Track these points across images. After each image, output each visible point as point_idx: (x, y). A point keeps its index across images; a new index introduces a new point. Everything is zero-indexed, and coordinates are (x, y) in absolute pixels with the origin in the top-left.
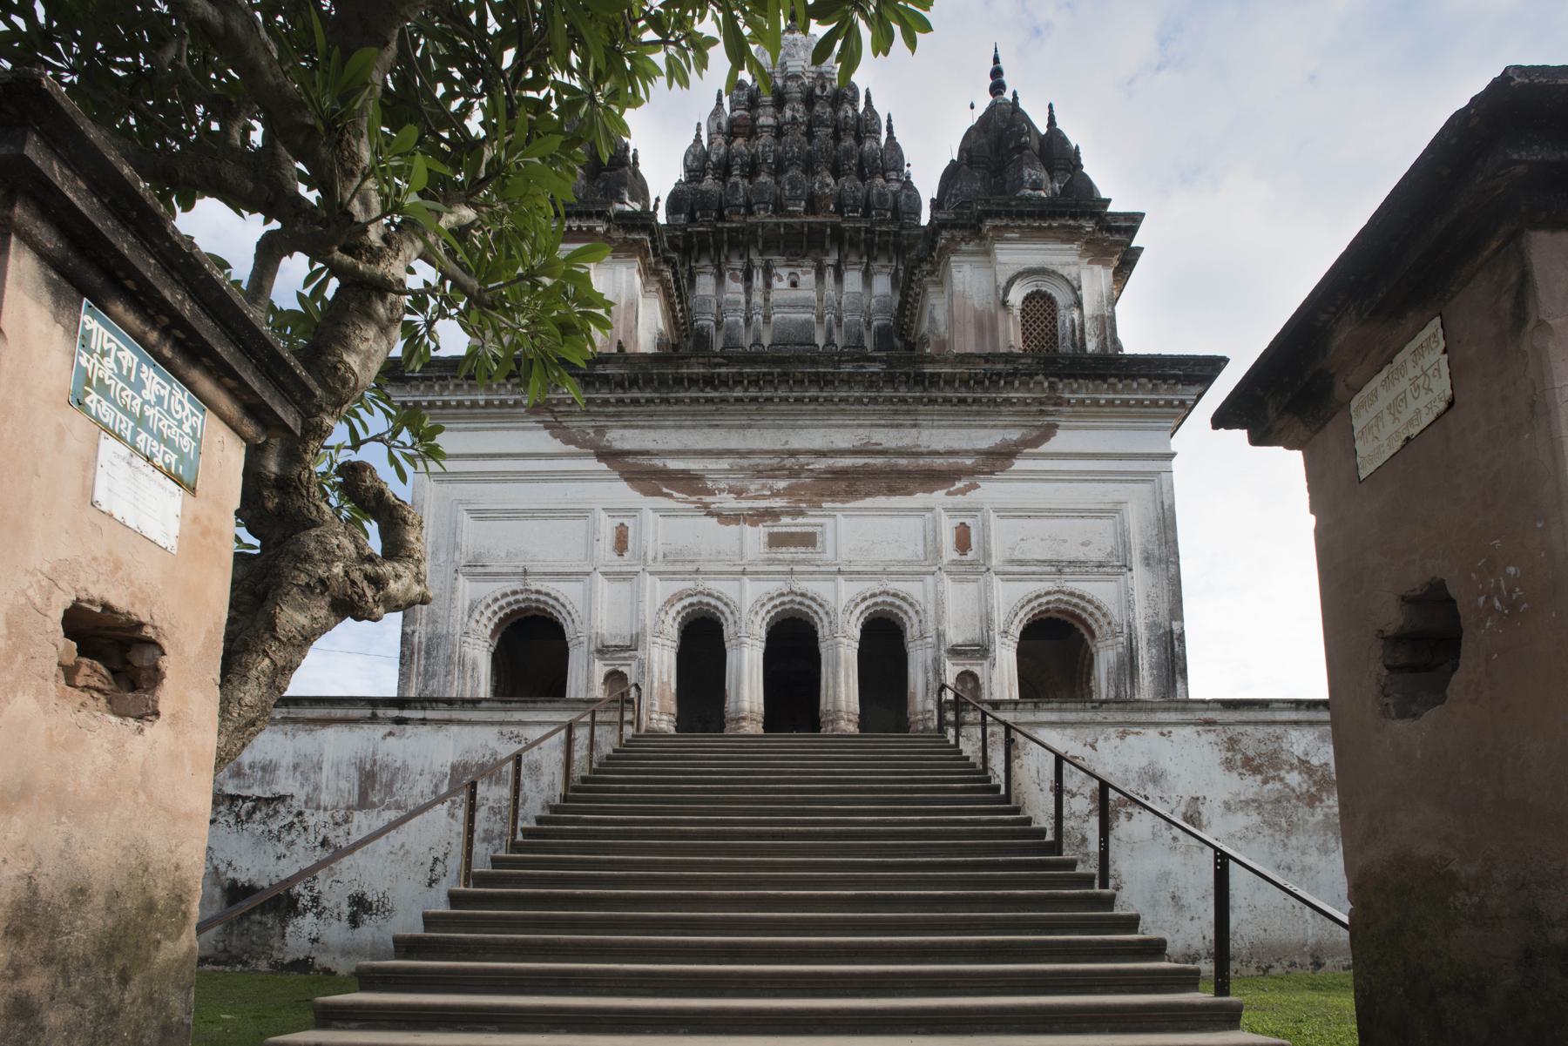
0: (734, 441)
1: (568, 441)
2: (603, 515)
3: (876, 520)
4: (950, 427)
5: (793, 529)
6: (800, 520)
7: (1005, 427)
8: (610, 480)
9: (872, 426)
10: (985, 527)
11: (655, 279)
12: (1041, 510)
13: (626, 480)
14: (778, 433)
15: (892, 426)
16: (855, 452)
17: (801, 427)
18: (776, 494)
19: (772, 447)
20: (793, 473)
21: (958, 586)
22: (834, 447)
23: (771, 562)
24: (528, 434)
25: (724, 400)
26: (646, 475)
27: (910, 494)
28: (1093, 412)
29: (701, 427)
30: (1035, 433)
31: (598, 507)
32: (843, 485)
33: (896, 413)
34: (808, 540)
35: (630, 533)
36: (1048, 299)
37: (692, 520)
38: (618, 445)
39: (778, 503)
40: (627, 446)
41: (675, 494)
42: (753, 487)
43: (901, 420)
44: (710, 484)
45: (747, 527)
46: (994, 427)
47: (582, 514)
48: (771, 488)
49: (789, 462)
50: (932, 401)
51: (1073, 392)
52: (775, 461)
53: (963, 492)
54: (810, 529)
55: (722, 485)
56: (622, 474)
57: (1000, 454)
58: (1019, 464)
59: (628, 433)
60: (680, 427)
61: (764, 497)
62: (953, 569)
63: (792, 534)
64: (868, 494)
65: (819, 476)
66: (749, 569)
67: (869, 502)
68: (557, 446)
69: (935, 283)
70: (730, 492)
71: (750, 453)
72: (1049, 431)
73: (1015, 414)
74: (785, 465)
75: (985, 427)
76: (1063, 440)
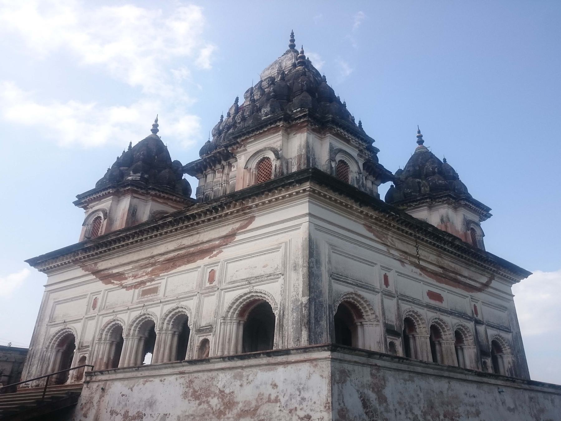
3: (180, 276)
4: (211, 230)
5: (151, 287)
7: (233, 223)
8: (97, 281)
12: (245, 256)
13: (101, 280)
18: (147, 274)
21: (206, 299)
23: (139, 303)
32: (171, 264)
39: (146, 277)
41: (115, 282)
42: (140, 273)
46: (228, 225)
53: (215, 255)
54: (156, 286)
56: (100, 278)
58: (238, 238)
62: (204, 291)
64: (180, 266)
65: (162, 263)
66: (130, 307)
75: (225, 225)
76: (257, 223)
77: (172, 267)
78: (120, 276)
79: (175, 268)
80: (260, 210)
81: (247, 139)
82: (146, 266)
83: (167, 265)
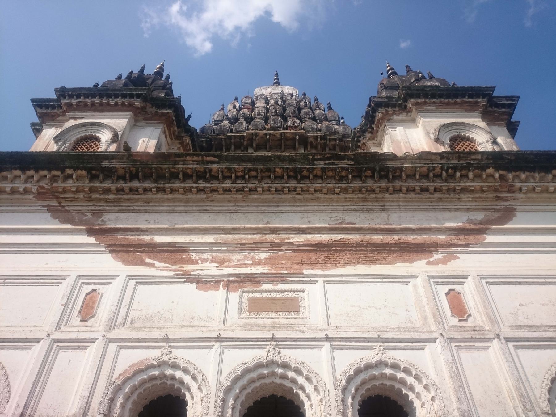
4: (415, 211)
5: (274, 295)
6: (281, 286)
7: (468, 210)
9: (345, 210)
15: (362, 211)
20: (273, 246)
29: (192, 211)
33: (365, 200)
43: (369, 205)
44: (193, 255)
46: (457, 210)
48: (253, 258)
49: (270, 238)
50: (396, 191)
52: (257, 237)
54: (292, 295)
60: (173, 211)
61: (246, 266)
63: (273, 300)
64: (347, 264)
65: (297, 248)
70: (212, 261)
72: (507, 214)
73: (475, 200)
75: (449, 210)
77: (326, 262)
79: (337, 267)
82: (255, 247)
83: (313, 256)
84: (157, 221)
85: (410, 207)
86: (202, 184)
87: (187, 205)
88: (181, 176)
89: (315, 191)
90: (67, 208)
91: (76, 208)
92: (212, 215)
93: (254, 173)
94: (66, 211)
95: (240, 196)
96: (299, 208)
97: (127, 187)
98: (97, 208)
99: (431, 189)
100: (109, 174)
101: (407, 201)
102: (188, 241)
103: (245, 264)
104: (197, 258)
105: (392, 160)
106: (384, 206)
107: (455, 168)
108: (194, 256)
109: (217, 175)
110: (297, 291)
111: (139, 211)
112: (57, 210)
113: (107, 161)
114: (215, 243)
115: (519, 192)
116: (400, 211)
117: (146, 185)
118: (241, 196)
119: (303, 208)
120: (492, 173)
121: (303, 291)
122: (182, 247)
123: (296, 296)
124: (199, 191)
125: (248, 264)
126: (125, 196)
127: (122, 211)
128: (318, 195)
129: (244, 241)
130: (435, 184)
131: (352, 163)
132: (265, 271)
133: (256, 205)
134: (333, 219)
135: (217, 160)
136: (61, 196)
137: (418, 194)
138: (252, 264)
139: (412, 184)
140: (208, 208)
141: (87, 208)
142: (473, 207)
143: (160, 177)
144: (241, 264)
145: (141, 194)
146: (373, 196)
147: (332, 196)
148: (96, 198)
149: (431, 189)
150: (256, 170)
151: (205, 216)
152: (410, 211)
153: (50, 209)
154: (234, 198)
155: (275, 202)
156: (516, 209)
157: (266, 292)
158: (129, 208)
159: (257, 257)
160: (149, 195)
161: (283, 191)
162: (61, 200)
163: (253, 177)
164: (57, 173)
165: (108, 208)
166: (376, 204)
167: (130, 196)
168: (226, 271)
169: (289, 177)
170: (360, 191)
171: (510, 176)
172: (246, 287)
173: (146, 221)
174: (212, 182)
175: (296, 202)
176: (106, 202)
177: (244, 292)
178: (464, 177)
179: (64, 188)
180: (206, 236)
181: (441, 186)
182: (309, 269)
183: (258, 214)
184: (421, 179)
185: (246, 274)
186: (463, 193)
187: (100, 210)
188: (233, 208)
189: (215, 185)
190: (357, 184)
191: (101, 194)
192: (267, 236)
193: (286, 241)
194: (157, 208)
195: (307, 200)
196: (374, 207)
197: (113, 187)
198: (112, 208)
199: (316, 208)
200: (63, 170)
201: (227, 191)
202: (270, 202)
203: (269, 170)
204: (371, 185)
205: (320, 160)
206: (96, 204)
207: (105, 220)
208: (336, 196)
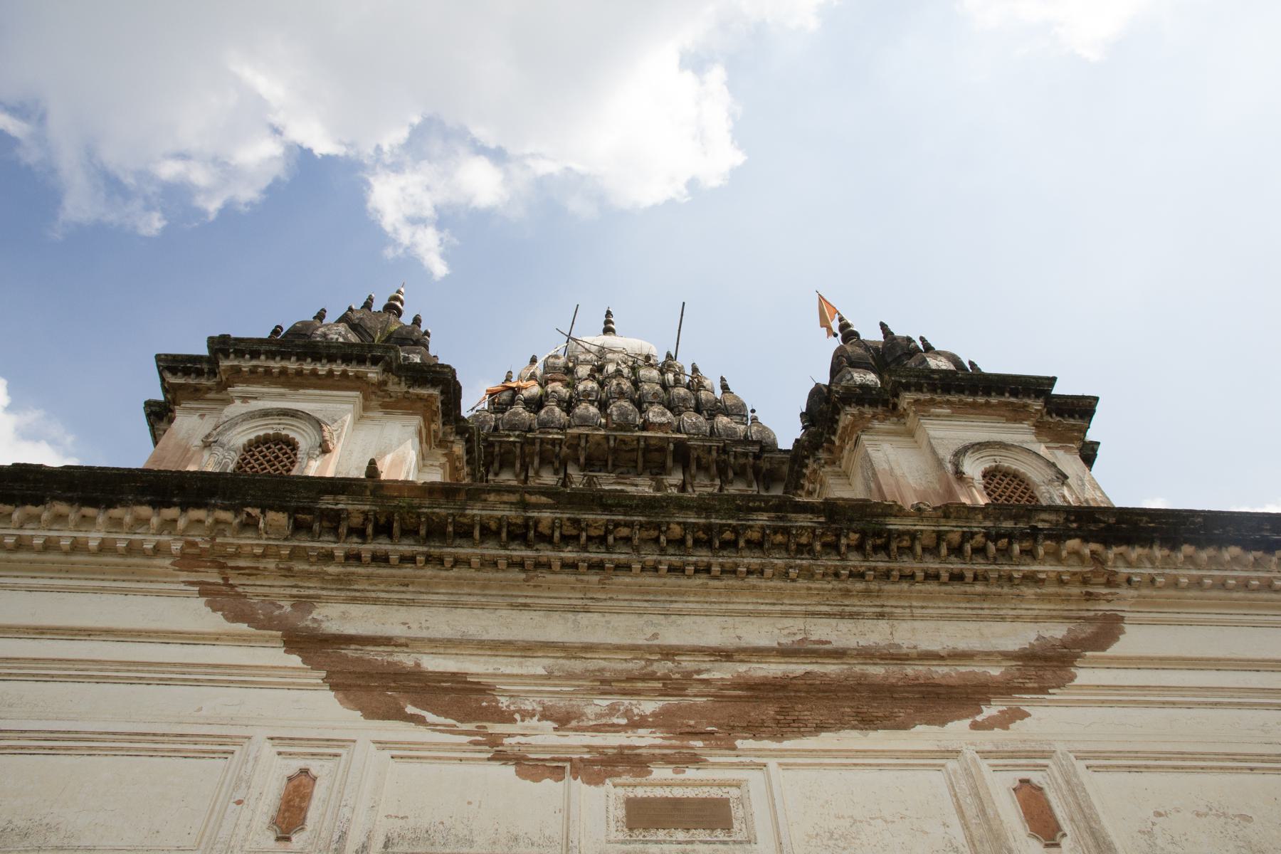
0: (557, 629)
1: (235, 616)
2: (269, 750)
4: (942, 617)
5: (678, 793)
6: (691, 773)
7: (1036, 619)
10: (1073, 788)
11: (440, 452)
13: (334, 687)
14: (640, 621)
15: (842, 616)
16: (785, 653)
17: (680, 614)
18: (636, 723)
19: (627, 641)
20: (671, 687)
22: (743, 644)
24: (163, 602)
25: (538, 565)
26: (377, 684)
27: (904, 726)
28: (1171, 598)
30: (1089, 630)
31: (260, 734)
32: (771, 710)
33: (847, 593)
34: (711, 815)
35: (319, 792)
36: (1015, 476)
37: (463, 768)
38: (332, 627)
39: (645, 739)
40: (350, 630)
41: (430, 717)
42: (590, 711)
43: (855, 604)
44: (504, 702)
45: (578, 786)
46: (1017, 618)
47: (221, 746)
48: (627, 713)
49: (662, 667)
51: (1129, 564)
52: (635, 666)
54: (715, 793)
55: (528, 706)
57: (1046, 659)
58: (1084, 676)
59: (356, 610)
60: (455, 605)
61: (615, 728)
63: (677, 803)
64: (820, 728)
67: (827, 740)
68: (215, 622)
69: (838, 475)
70: (544, 717)
71: (589, 648)
72: (1109, 630)
74: (660, 673)
75: (1003, 619)
76: (1133, 640)
77: (778, 722)
78: (463, 699)
79: (803, 735)
80: (1141, 601)
81: (932, 402)
84: (424, 625)
85: (930, 611)
86: (519, 552)
87: (487, 592)
88: (477, 533)
89: (749, 572)
90: (240, 590)
91: (260, 590)
92: (537, 616)
93: (624, 532)
94: (239, 594)
95: (594, 578)
96: (716, 606)
97: (367, 550)
98: (303, 592)
99: (969, 575)
100: (333, 521)
101: (924, 599)
102: (491, 671)
103: (613, 725)
104: (512, 708)
105: (896, 516)
106: (883, 606)
107: (1010, 536)
108: (506, 704)
109: (547, 532)
110: (725, 785)
111: (387, 602)
112: (219, 593)
113: (331, 497)
114: (549, 676)
115: (1125, 585)
116: (913, 618)
117: (406, 547)
118: (595, 578)
119: (724, 606)
120: (1076, 547)
121: (738, 786)
122: (479, 683)
123: (725, 796)
124: (512, 564)
125: (619, 725)
126: (360, 570)
127: (354, 600)
128: (753, 580)
129: (607, 675)
130: (976, 567)
131: (822, 519)
132: (658, 741)
133: (627, 597)
134: (786, 632)
135: (550, 501)
136: (231, 564)
137: (945, 584)
138: (626, 725)
139: (932, 564)
140: (528, 601)
141: (281, 591)
142: (1045, 613)
143: (437, 532)
144: (604, 725)
145: (392, 567)
146: (860, 586)
147: (780, 584)
148: (302, 571)
149: (969, 575)
150: (629, 525)
151: (525, 616)
152: (932, 617)
153: (206, 590)
154: (582, 581)
155: (668, 594)
156: (1123, 618)
157: (661, 785)
158: (368, 594)
159: (636, 711)
160: (408, 570)
161: (683, 571)
162: (228, 571)
163: (622, 538)
164: (226, 516)
165: (324, 593)
166: (867, 602)
167: (370, 570)
168: (576, 740)
169: (698, 543)
170: (837, 575)
171: (1111, 553)
172: (619, 775)
173: (404, 624)
174: (538, 546)
175: (709, 594)
176: (323, 580)
177: (615, 786)
178: (1030, 554)
179: (239, 546)
180: (530, 662)
181: (986, 571)
182: (746, 738)
183: (633, 617)
184: (949, 555)
185: (621, 747)
186: (1027, 586)
187: (308, 597)
188: (580, 602)
189: (546, 553)
190: (832, 562)
191: (312, 564)
192: (655, 666)
193: (696, 677)
194: (425, 597)
195: (731, 590)
196: (864, 609)
197: (339, 550)
198: (334, 593)
199: (750, 607)
200: (237, 510)
201: (570, 566)
202: (656, 593)
203: (658, 526)
204: (857, 563)
205: (759, 509)
206: (301, 584)
207: (320, 618)
208: (790, 585)
